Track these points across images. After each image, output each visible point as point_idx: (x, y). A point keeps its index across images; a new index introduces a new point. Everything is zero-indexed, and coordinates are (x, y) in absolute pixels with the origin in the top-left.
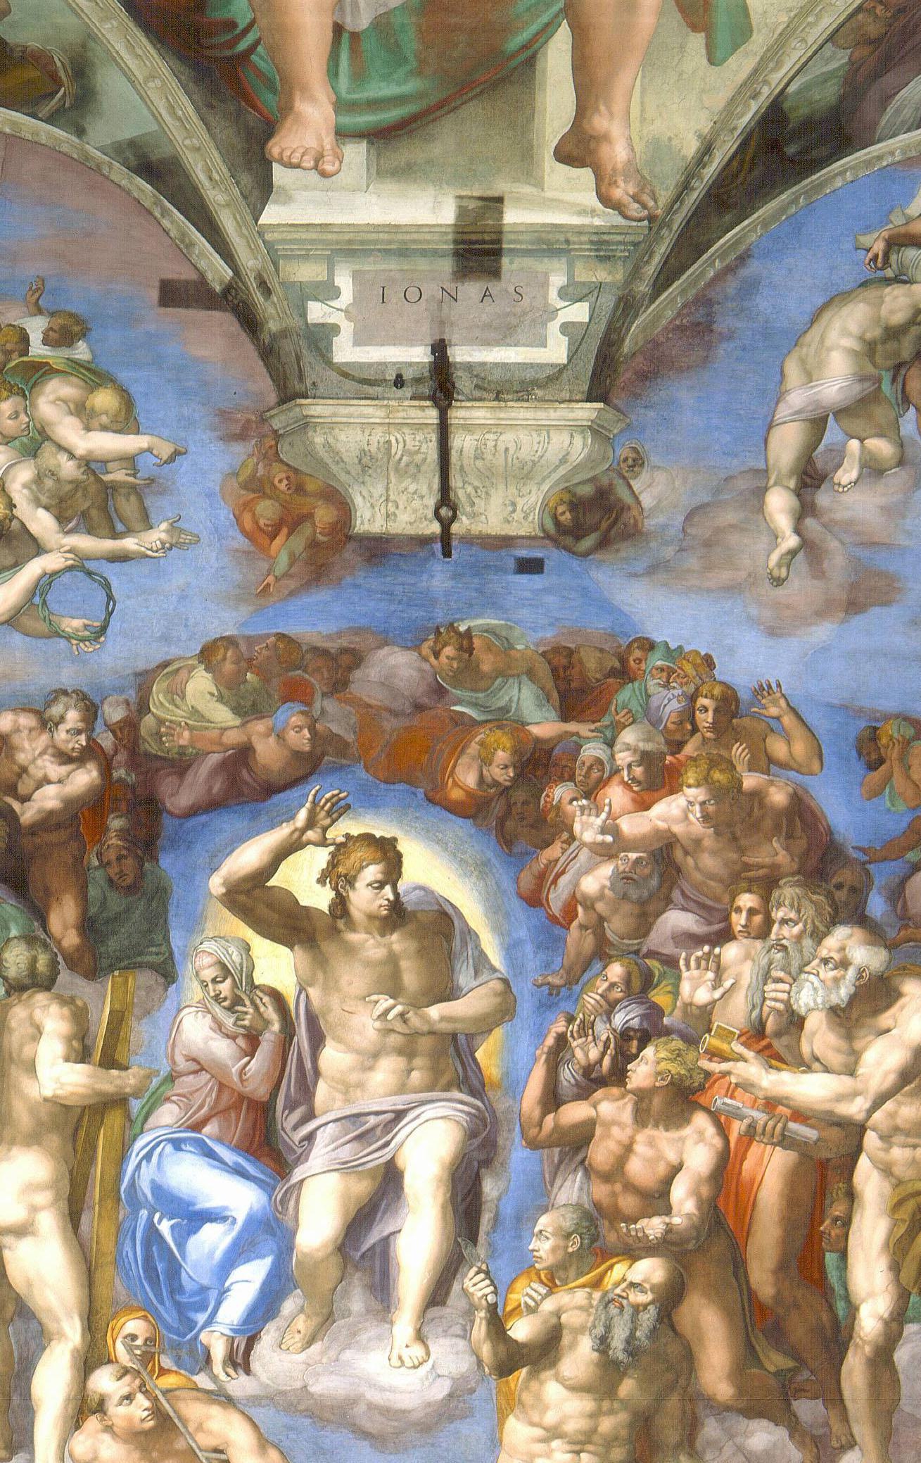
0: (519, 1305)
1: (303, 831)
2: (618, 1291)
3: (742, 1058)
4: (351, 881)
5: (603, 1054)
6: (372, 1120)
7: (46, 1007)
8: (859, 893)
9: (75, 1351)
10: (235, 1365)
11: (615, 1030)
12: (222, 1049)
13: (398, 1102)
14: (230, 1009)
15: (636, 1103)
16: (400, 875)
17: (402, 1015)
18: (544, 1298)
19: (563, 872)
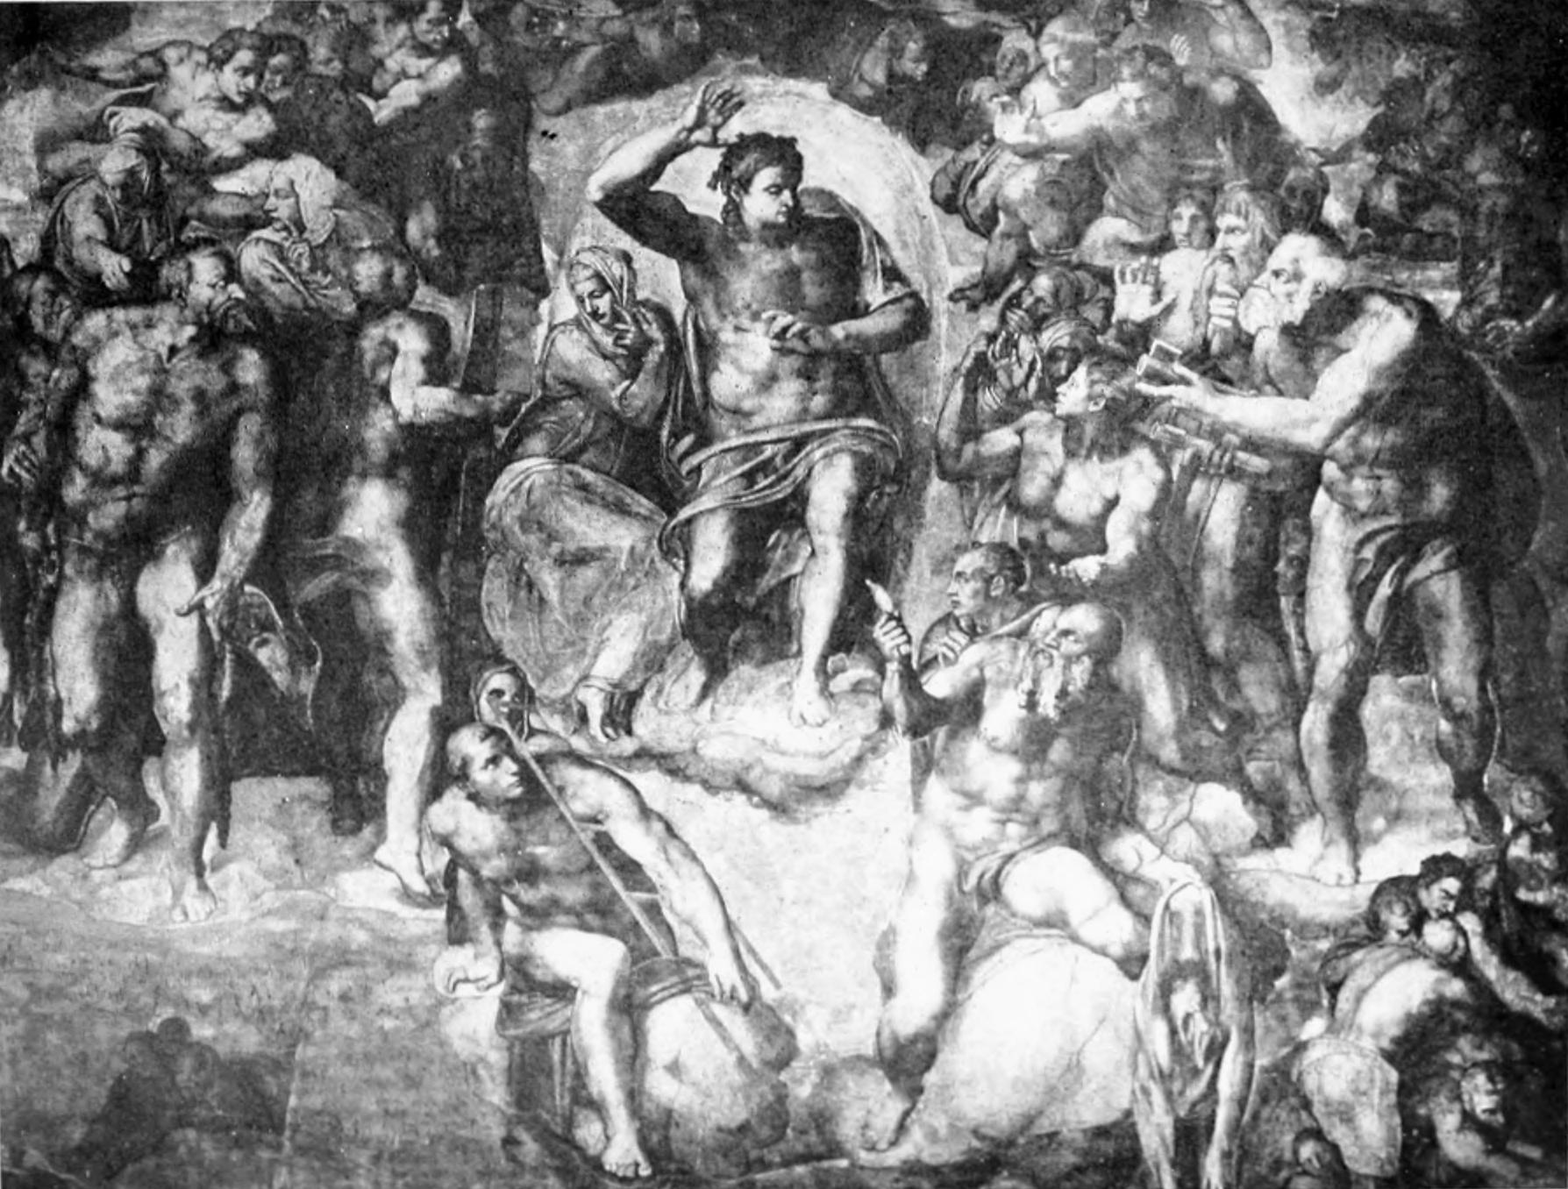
0: (936, 658)
1: (691, 130)
2: (1048, 640)
3: (1188, 383)
4: (745, 184)
5: (1028, 377)
6: (769, 451)
7: (400, 327)
8: (1314, 196)
9: (435, 712)
10: (615, 727)
11: (1041, 351)
12: (601, 373)
13: (797, 431)
14: (609, 328)
15: (1067, 430)
16: (799, 179)
17: (802, 335)
18: (964, 649)
19: (981, 176)
